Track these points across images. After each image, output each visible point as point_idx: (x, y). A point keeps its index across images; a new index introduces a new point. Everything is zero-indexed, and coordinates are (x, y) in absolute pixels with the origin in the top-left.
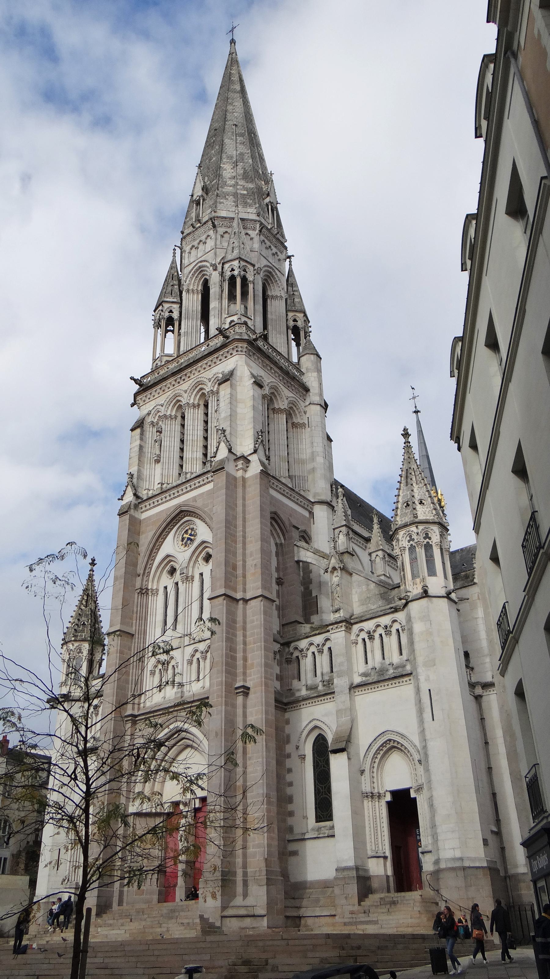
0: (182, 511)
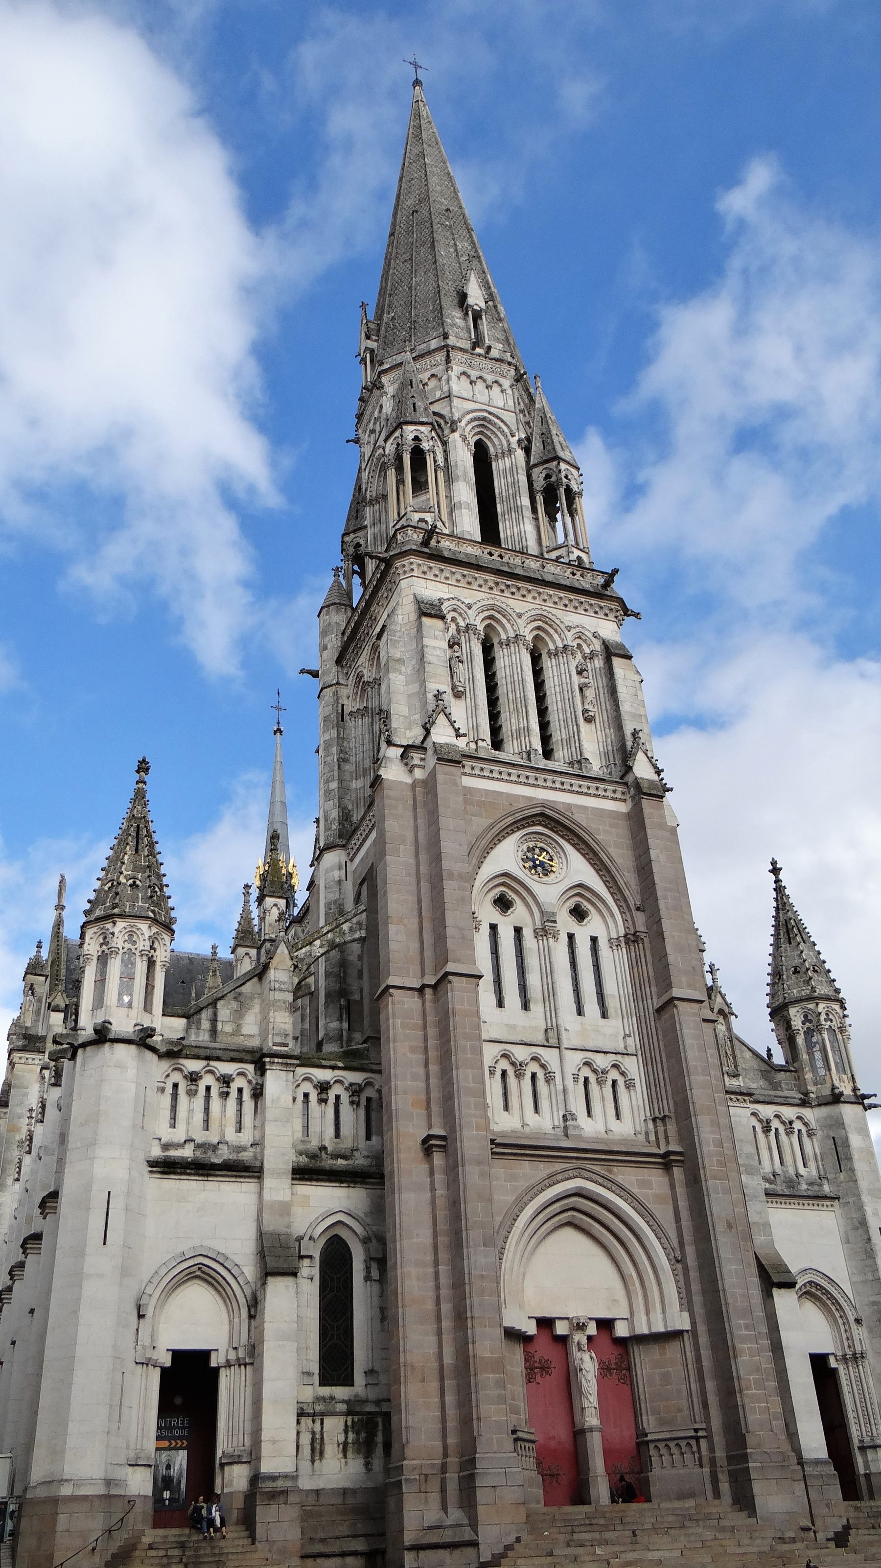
0: (542, 815)
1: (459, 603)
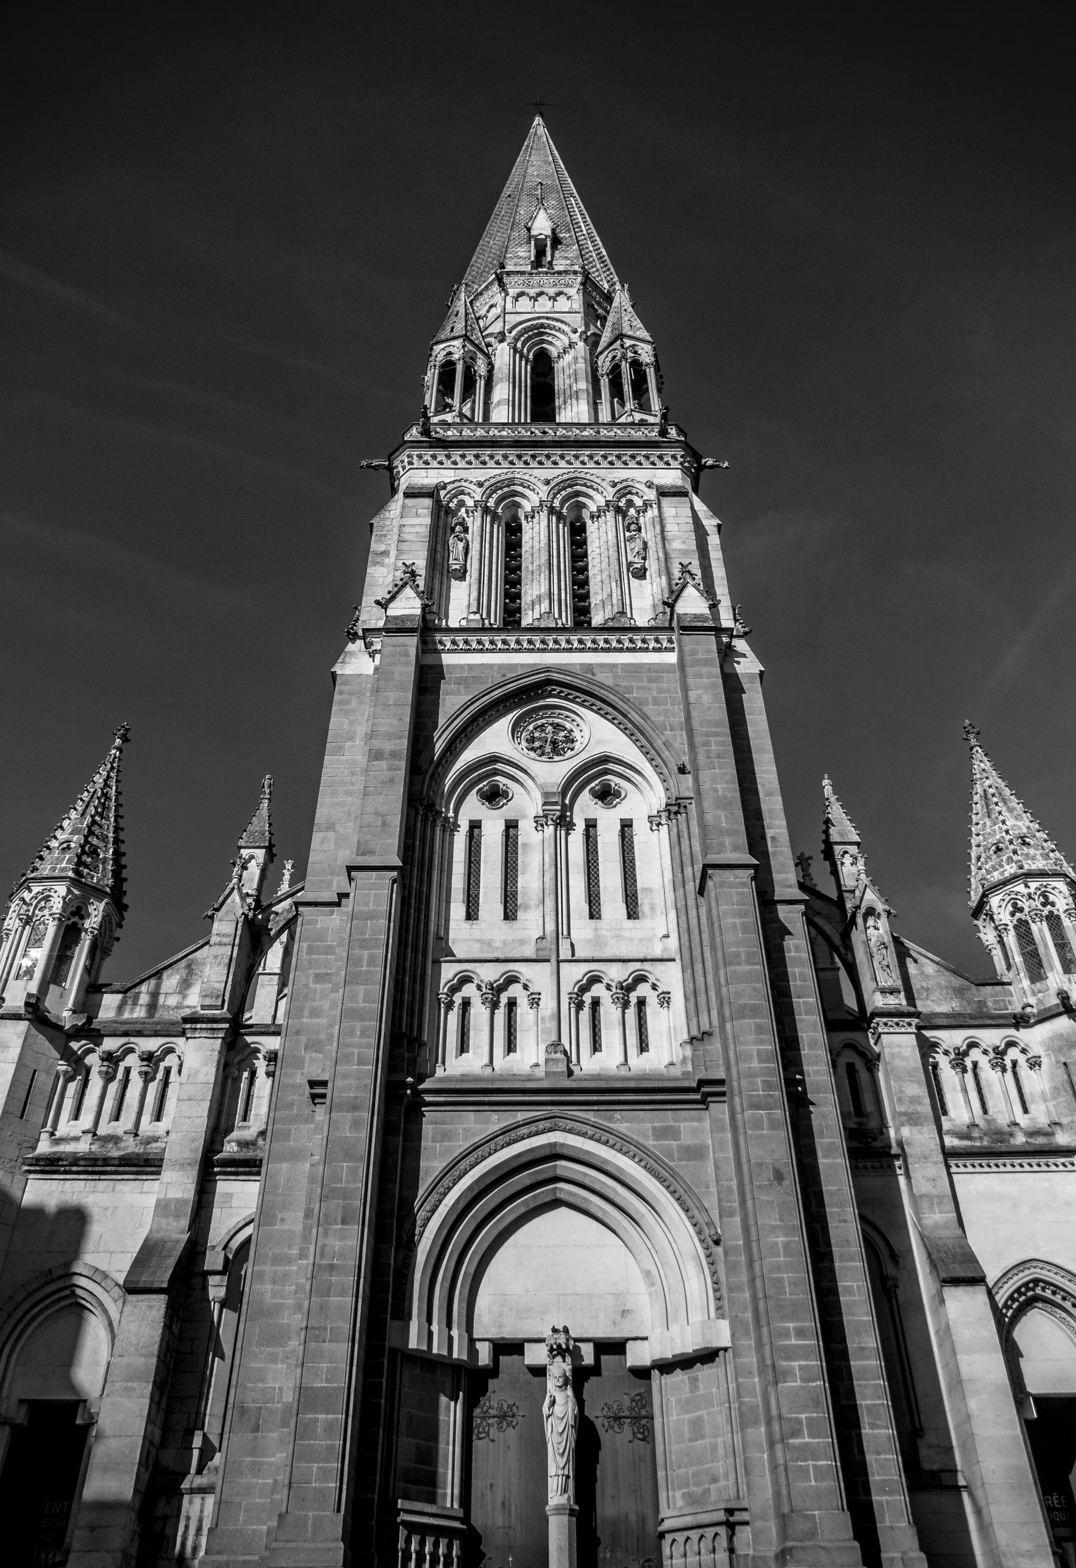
0: (549, 682)
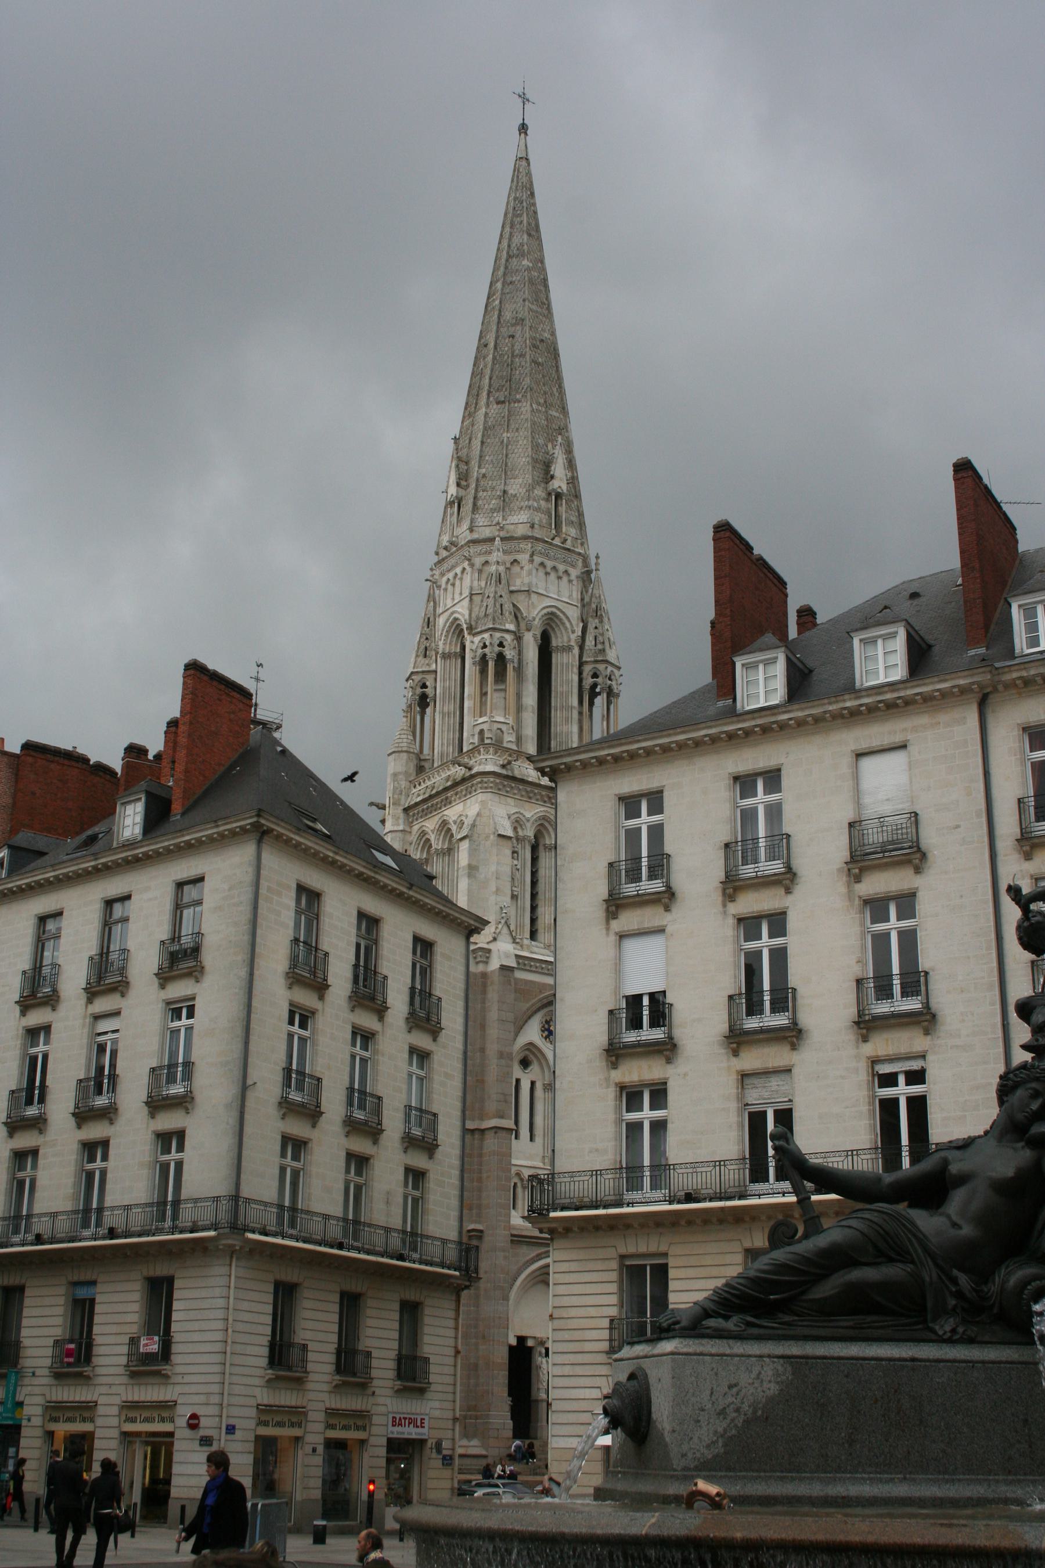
1: (521, 816)
